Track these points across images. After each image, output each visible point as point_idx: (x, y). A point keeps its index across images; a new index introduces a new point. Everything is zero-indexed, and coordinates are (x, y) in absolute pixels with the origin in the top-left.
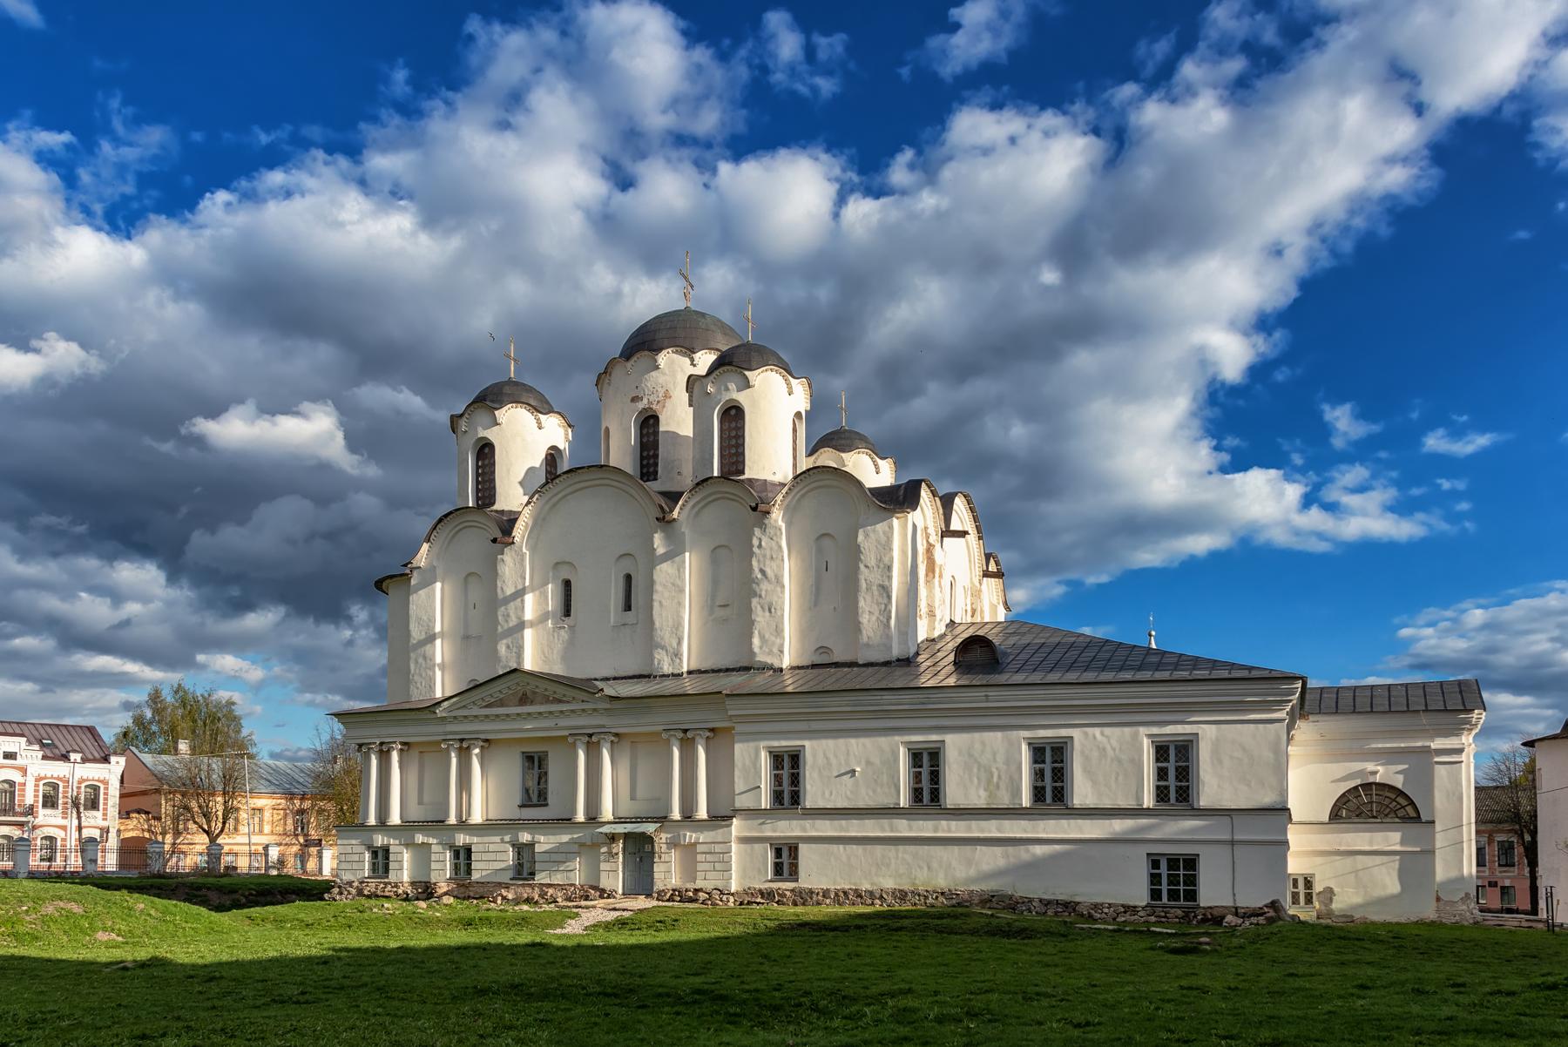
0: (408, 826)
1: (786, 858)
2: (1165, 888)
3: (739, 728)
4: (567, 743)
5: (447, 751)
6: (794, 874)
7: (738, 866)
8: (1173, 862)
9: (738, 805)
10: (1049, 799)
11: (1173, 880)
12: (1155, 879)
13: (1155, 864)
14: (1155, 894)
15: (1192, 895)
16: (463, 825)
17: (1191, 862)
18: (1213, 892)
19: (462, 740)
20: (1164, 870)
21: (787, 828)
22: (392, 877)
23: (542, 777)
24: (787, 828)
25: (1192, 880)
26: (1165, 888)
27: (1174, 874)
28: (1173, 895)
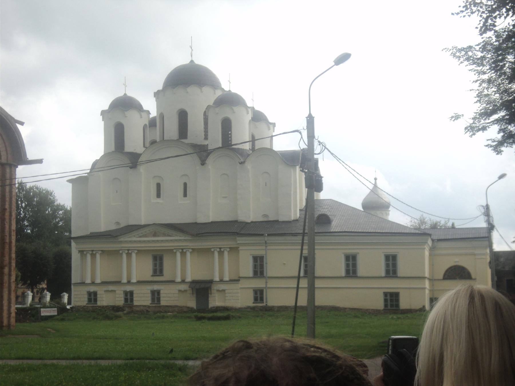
0: (104, 283)
1: (259, 295)
2: (389, 303)
3: (241, 248)
4: (171, 252)
5: (122, 254)
6: (262, 299)
7: (240, 297)
8: (392, 294)
9: (241, 275)
10: (351, 274)
11: (391, 300)
12: (386, 300)
13: (385, 294)
14: (386, 306)
15: (398, 305)
16: (93, 283)
17: (397, 295)
18: (404, 304)
19: (128, 250)
20: (388, 298)
21: (259, 284)
22: (99, 303)
23: (161, 264)
24: (259, 284)
25: (397, 300)
26: (389, 303)
27: (392, 299)
28: (392, 306)
